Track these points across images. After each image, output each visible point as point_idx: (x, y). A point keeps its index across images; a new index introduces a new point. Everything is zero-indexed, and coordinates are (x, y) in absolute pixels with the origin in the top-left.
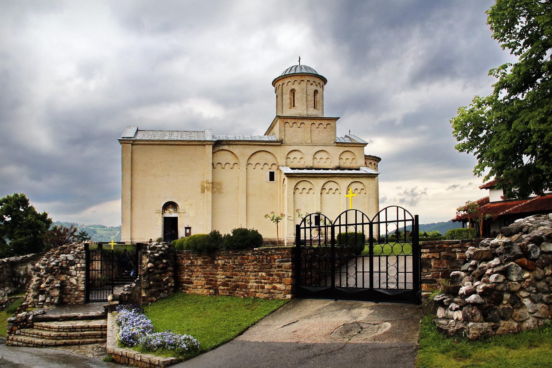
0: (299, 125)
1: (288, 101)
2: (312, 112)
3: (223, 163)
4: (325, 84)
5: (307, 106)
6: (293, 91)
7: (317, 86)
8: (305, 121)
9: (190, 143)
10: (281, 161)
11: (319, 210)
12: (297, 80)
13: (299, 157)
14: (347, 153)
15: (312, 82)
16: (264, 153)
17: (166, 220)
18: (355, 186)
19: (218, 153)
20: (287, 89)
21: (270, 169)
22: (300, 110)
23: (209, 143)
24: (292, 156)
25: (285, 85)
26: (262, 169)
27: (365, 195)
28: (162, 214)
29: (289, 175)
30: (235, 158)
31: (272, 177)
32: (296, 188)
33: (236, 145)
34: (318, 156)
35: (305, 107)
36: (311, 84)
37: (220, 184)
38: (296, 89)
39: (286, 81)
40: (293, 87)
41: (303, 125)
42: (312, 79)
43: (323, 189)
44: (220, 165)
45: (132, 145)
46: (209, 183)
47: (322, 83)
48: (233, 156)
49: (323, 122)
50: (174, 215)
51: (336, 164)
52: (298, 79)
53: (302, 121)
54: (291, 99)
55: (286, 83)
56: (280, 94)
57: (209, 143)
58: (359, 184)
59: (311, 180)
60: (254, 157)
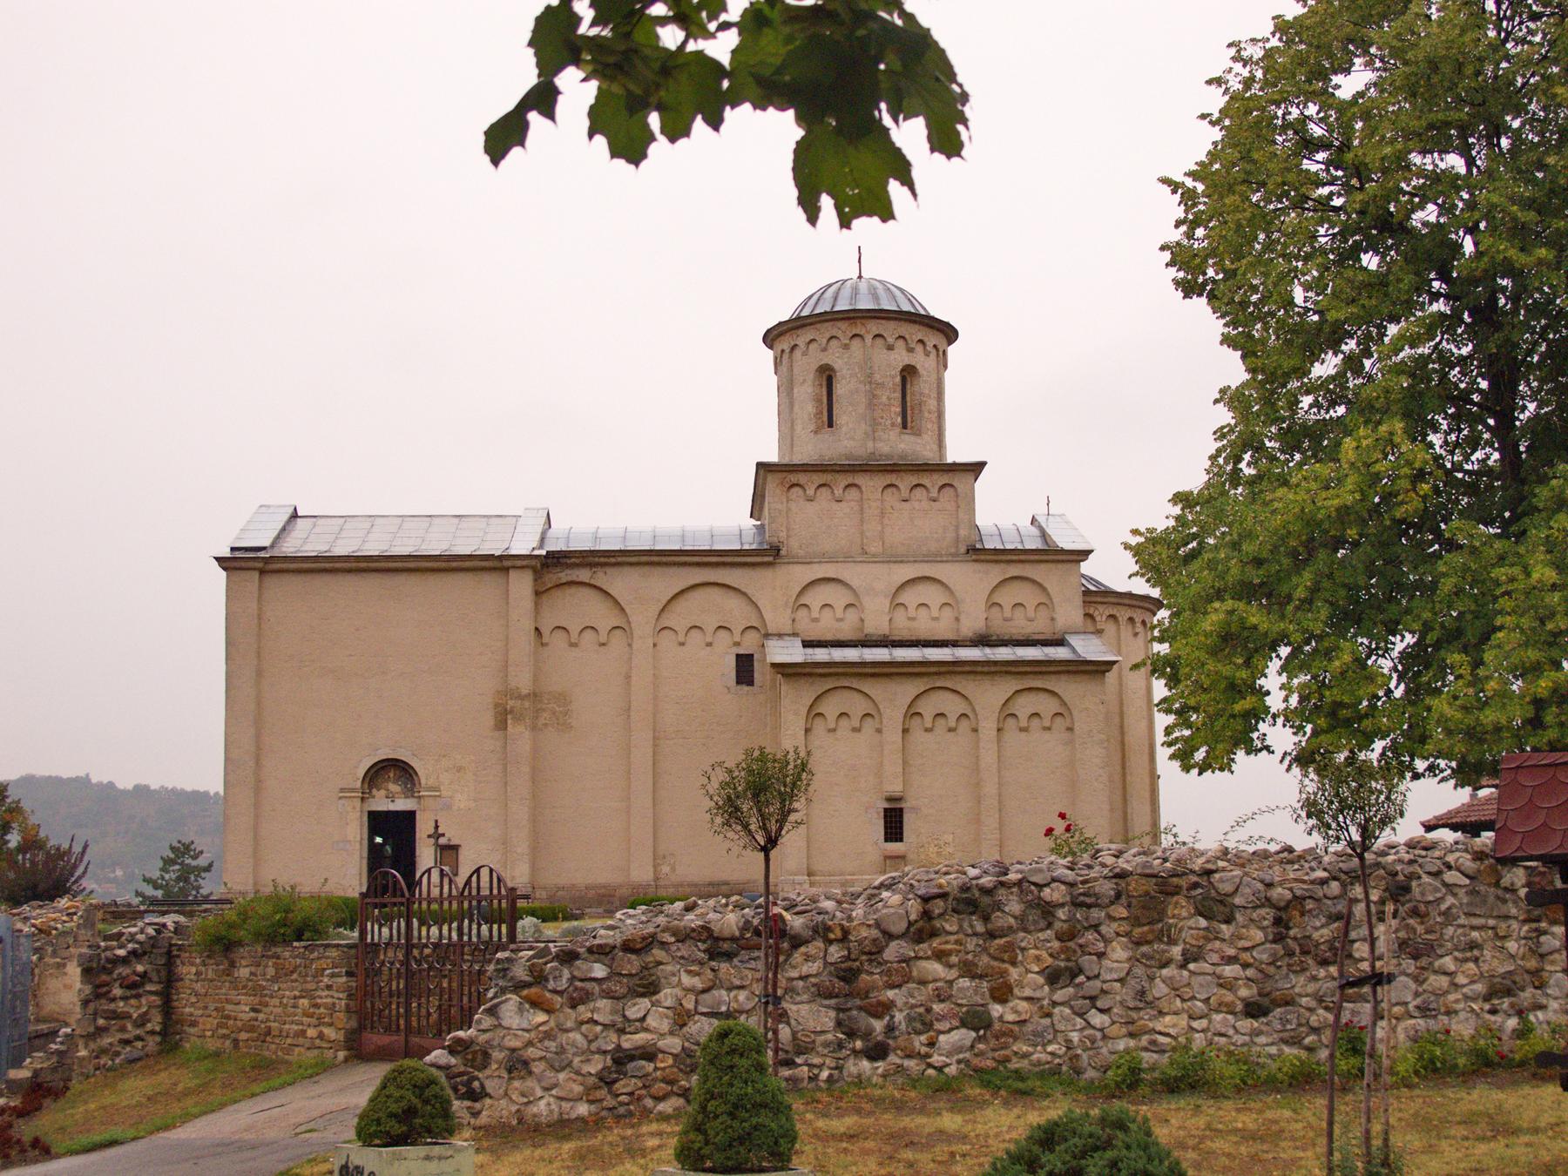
0: (838, 492)
1: (810, 408)
2: (896, 444)
3: (575, 629)
4: (950, 342)
5: (874, 424)
6: (827, 375)
7: (910, 350)
8: (860, 479)
9: (454, 564)
10: (776, 618)
11: (895, 788)
12: (839, 334)
14: (1016, 585)
15: (890, 340)
16: (715, 593)
17: (378, 822)
18: (1025, 705)
19: (558, 593)
20: (806, 364)
21: (737, 644)
22: (849, 440)
23: (519, 563)
24: (816, 598)
25: (798, 353)
26: (709, 644)
27: (1067, 735)
28: (363, 799)
29: (786, 671)
30: (616, 611)
31: (745, 668)
32: (813, 714)
34: (910, 597)
35: (869, 429)
36: (890, 348)
37: (563, 698)
38: (836, 367)
39: (802, 338)
40: (827, 359)
41: (853, 494)
42: (890, 330)
43: (912, 713)
44: (560, 633)
45: (262, 572)
46: (521, 697)
47: (933, 339)
49: (925, 480)
50: (401, 805)
51: (972, 623)
53: (850, 479)
54: (819, 401)
55: (802, 345)
57: (519, 563)
58: (1042, 696)
59: (867, 686)
60: (682, 605)
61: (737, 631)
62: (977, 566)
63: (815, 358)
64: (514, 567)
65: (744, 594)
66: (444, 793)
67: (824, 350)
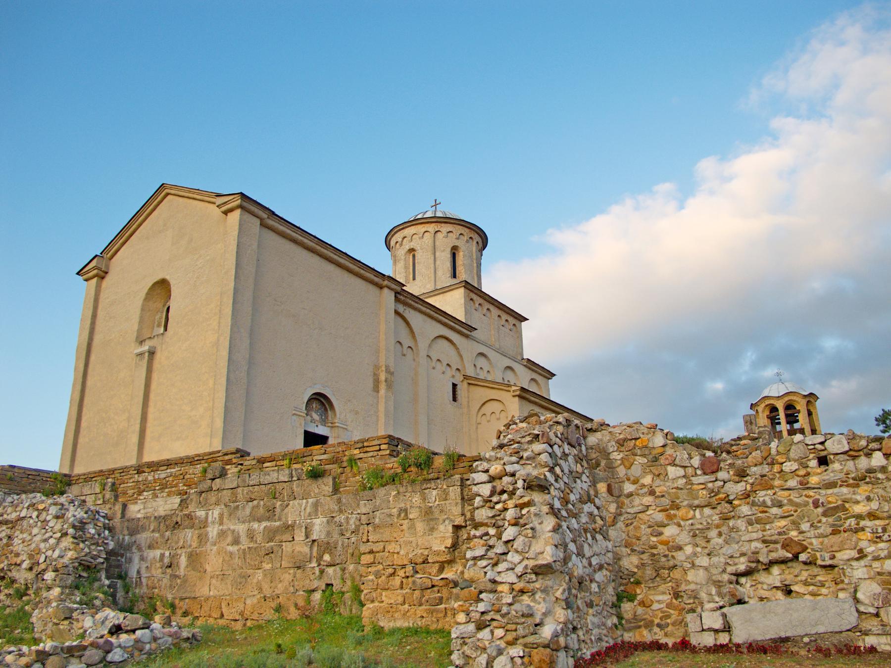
8: (492, 308)
13: (486, 369)
26: (443, 373)
33: (415, 309)
41: (488, 314)
45: (263, 225)
48: (407, 330)
50: (321, 430)
52: (465, 231)
56: (431, 249)
61: (454, 367)
62: (527, 370)
63: (452, 240)
64: (389, 288)
65: (457, 349)
66: (349, 428)
67: (458, 239)
